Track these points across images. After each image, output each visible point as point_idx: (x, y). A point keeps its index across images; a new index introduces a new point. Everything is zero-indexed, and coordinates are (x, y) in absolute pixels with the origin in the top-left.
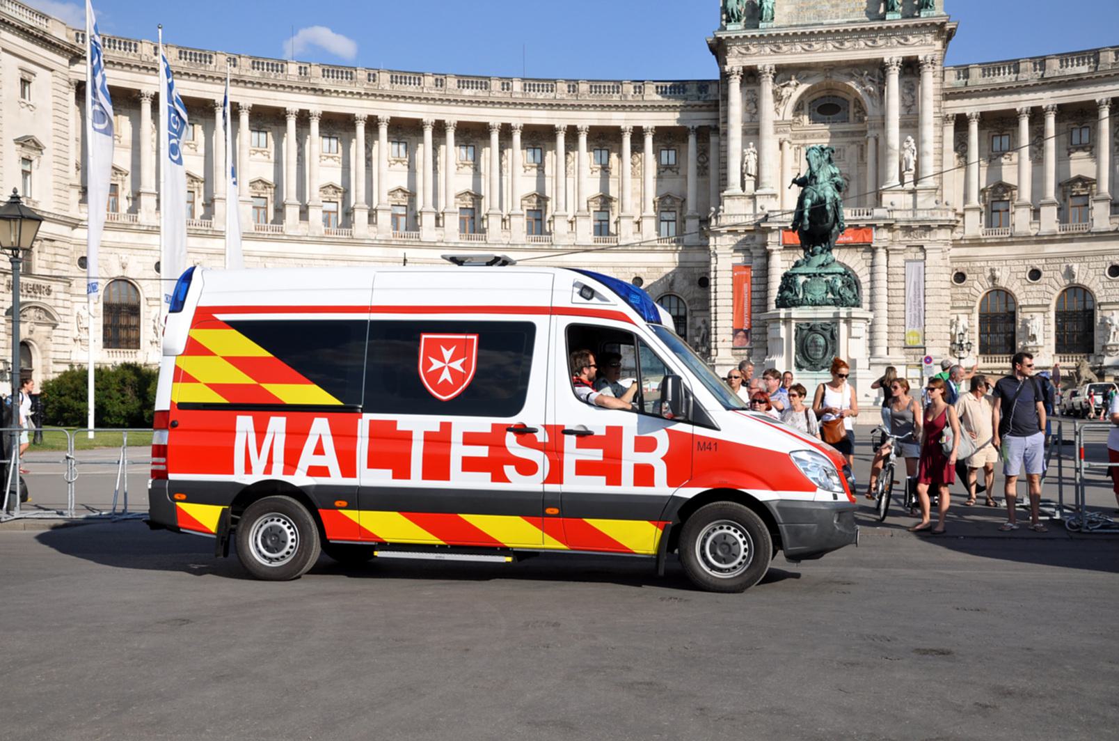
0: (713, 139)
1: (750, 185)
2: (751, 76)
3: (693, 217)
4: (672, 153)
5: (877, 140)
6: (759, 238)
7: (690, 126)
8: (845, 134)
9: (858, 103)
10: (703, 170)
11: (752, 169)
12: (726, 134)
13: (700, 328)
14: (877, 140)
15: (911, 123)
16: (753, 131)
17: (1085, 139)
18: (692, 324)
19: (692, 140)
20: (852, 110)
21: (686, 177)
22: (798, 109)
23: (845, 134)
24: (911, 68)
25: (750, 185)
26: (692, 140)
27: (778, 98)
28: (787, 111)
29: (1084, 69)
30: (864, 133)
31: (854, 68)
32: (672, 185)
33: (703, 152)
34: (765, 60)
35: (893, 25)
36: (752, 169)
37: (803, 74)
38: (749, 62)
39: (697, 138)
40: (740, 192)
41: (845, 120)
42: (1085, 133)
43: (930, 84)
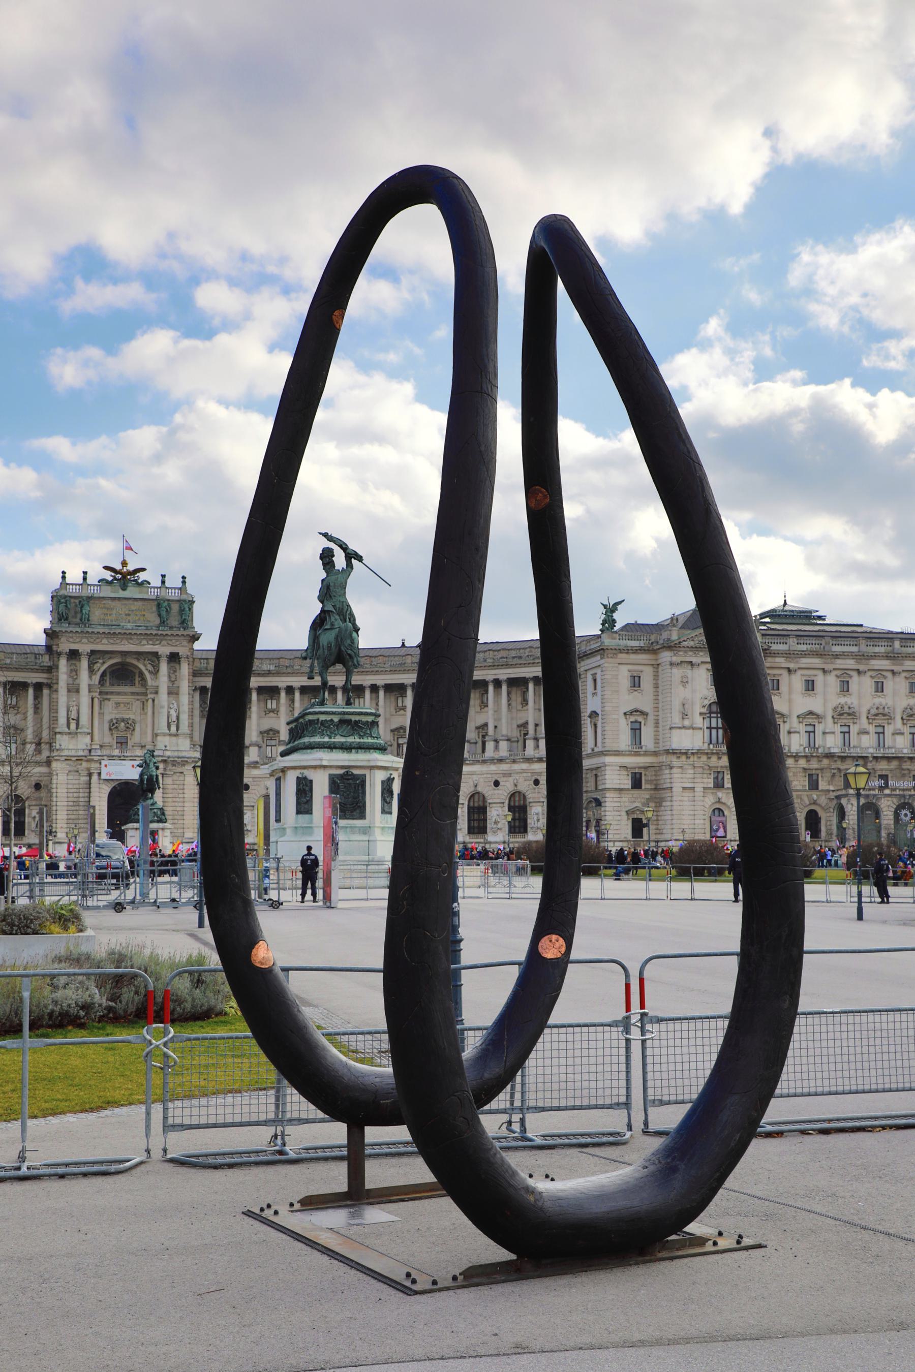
0: (46, 692)
1: (73, 726)
2: (74, 655)
3: (31, 743)
4: (14, 699)
5: (153, 701)
6: (85, 764)
7: (29, 681)
8: (133, 694)
9: (141, 674)
10: (37, 709)
11: (74, 715)
12: (56, 691)
13: (34, 817)
14: (153, 701)
15: (173, 692)
16: (74, 689)
17: (274, 706)
18: (29, 814)
19: (31, 691)
20: (137, 679)
21: (25, 714)
22: (103, 675)
23: (133, 694)
24: (174, 658)
25: (73, 726)
26: (31, 691)
27: (91, 671)
28: (96, 678)
29: (272, 668)
30: (146, 694)
31: (139, 655)
32: (14, 719)
33: (38, 697)
34: (85, 647)
35: (164, 633)
36: (74, 715)
37: (107, 656)
38: (74, 647)
39: (34, 690)
40: (67, 730)
41: (133, 684)
42: (274, 702)
43: (185, 669)
